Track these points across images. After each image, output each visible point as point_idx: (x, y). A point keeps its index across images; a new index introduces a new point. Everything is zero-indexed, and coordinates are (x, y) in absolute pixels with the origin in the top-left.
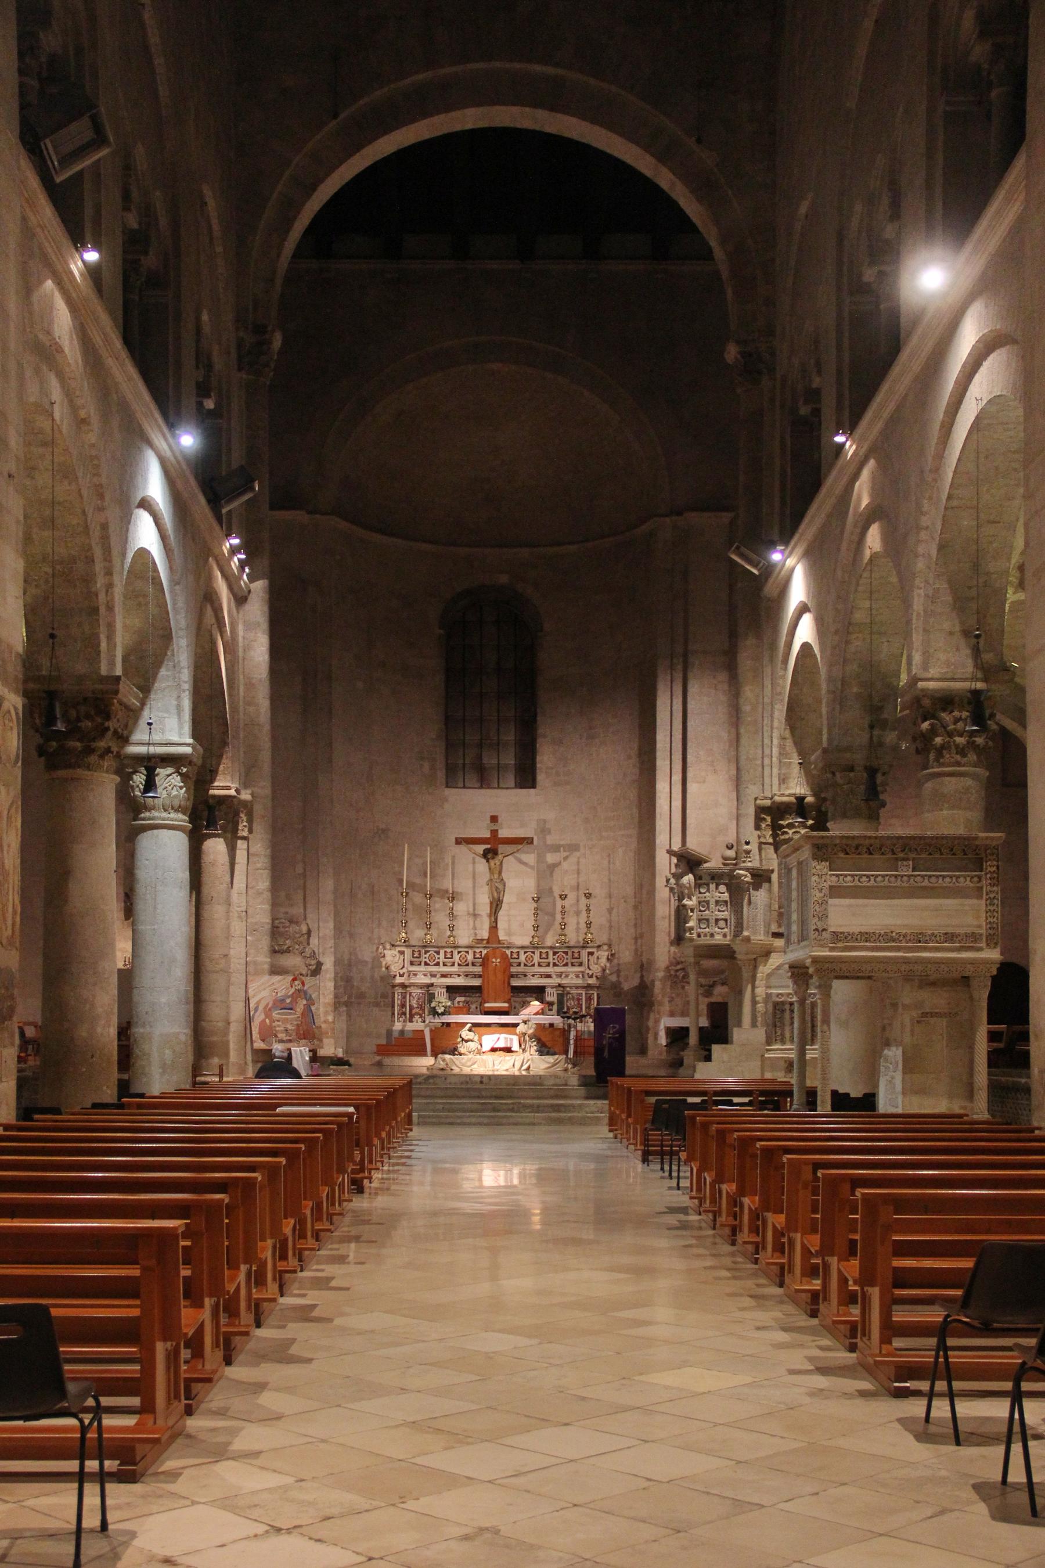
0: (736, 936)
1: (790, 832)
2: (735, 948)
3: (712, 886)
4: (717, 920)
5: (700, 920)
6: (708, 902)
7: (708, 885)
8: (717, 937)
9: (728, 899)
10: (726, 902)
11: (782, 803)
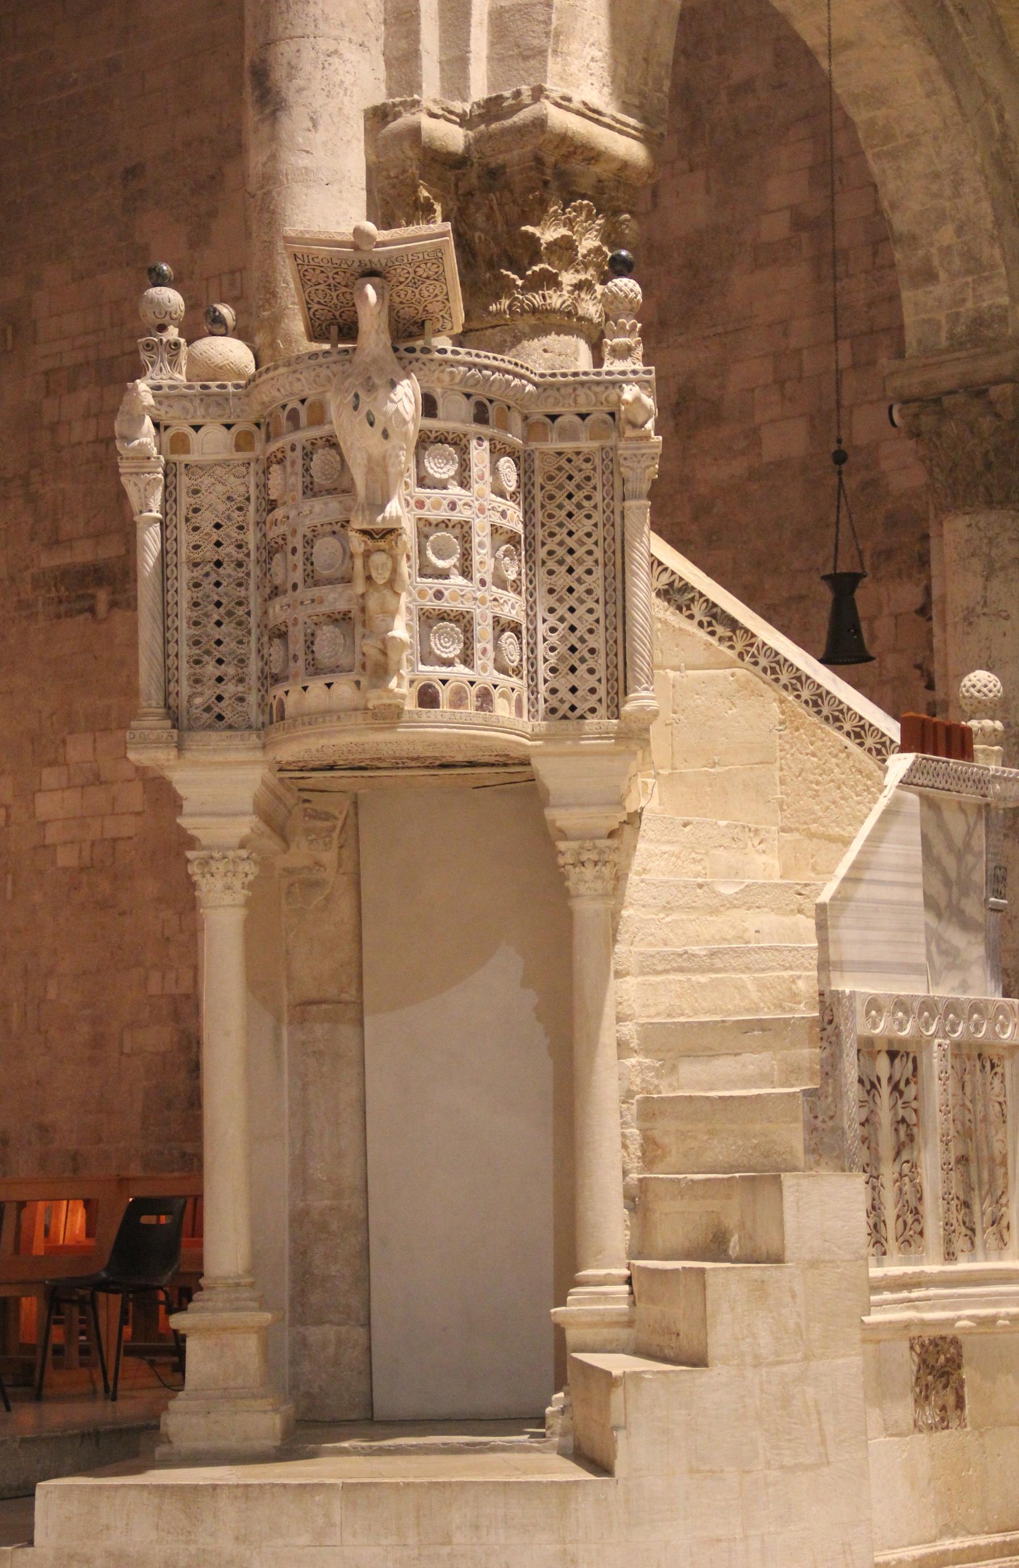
0: (564, 712)
1: (568, 278)
2: (546, 769)
3: (479, 455)
4: (501, 626)
5: (429, 619)
6: (464, 532)
7: (460, 444)
8: (502, 709)
9: (520, 528)
10: (513, 539)
11: (564, 139)
